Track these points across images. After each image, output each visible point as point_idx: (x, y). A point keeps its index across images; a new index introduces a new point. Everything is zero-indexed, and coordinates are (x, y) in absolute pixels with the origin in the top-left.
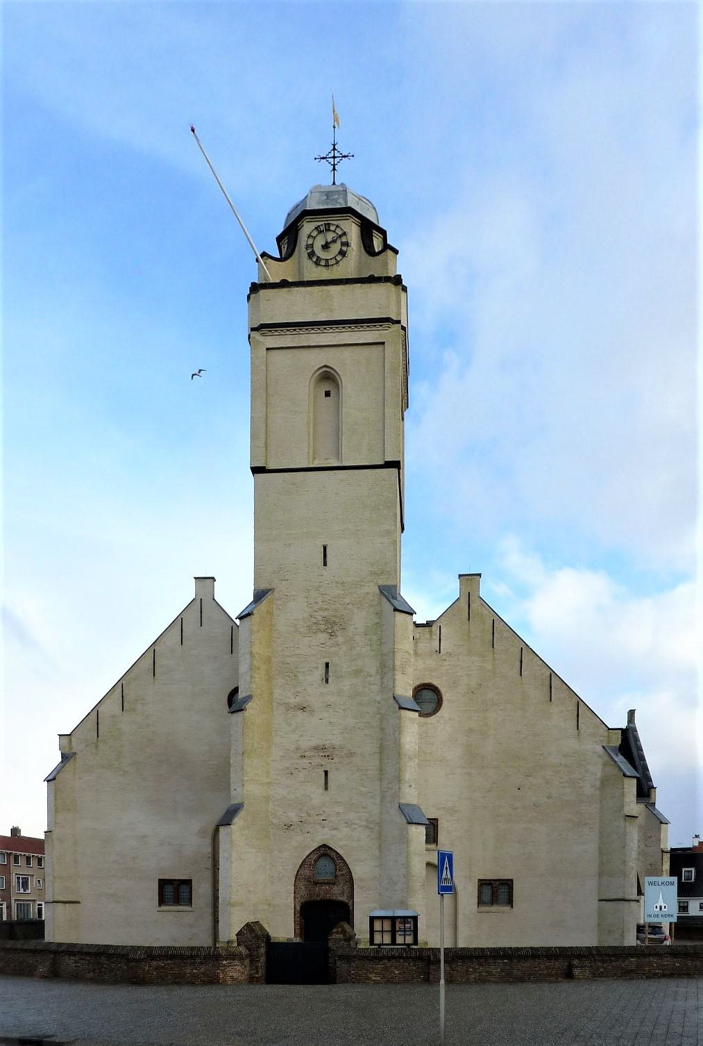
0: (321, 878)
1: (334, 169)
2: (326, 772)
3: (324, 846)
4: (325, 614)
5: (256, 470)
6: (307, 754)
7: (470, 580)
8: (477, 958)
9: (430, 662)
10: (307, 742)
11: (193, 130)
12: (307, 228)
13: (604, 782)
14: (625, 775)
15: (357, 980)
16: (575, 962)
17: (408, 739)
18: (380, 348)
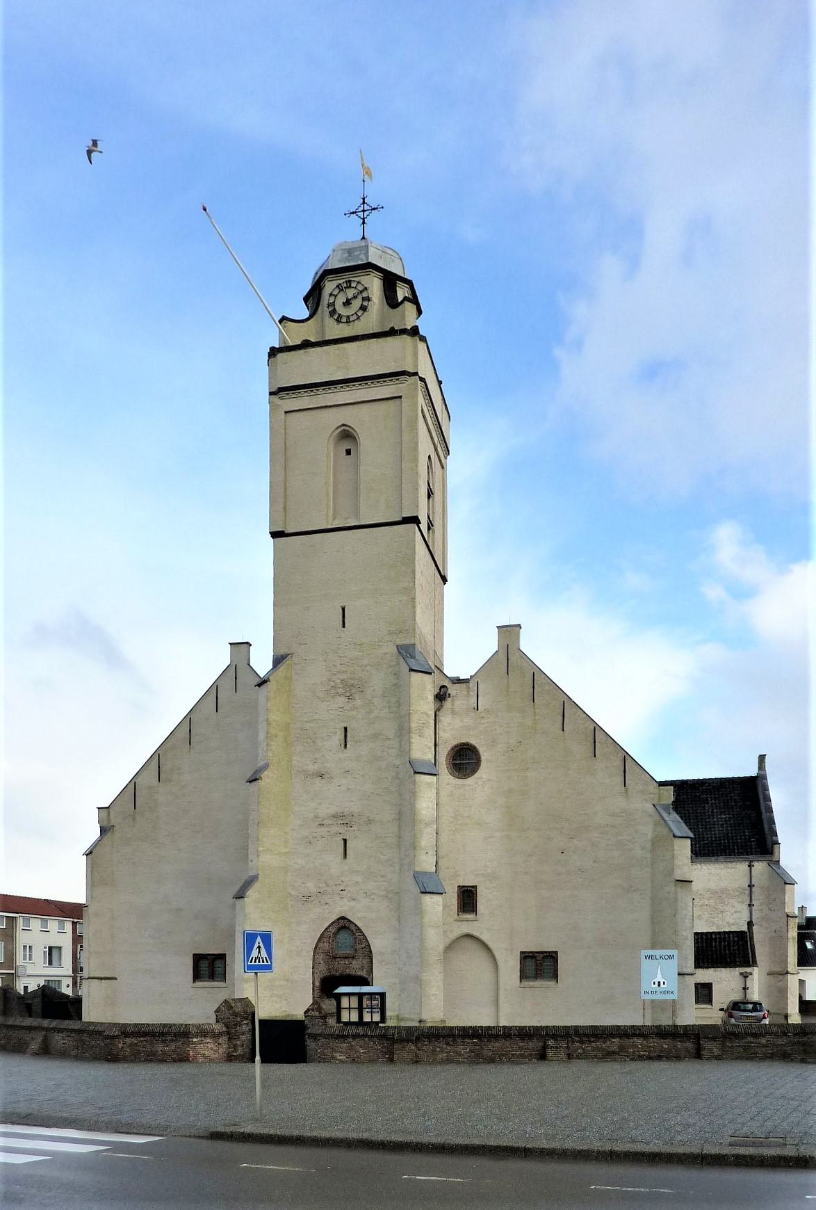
0: (340, 953)
2: (345, 840)
3: (343, 918)
4: (342, 677)
5: (275, 535)
6: (325, 822)
7: (509, 633)
8: (444, 1036)
10: (326, 810)
12: (330, 286)
13: (656, 843)
14: (674, 836)
15: (323, 1060)
16: (551, 1042)
17: (424, 805)
18: (398, 401)
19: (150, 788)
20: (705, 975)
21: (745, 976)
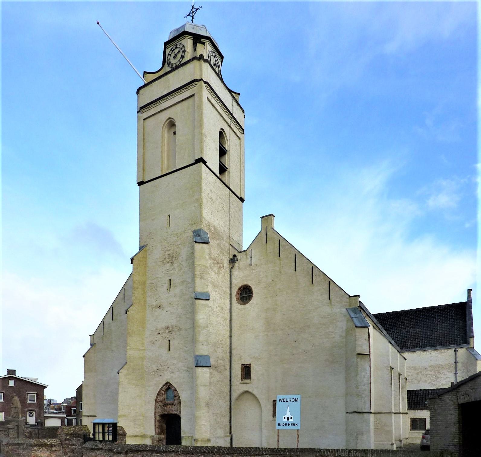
0: (168, 402)
2: (169, 341)
4: (168, 253)
5: (140, 184)
6: (161, 332)
7: (267, 219)
9: (246, 272)
10: (161, 326)
11: (98, 23)
13: (348, 332)
17: (201, 317)
19: (109, 324)
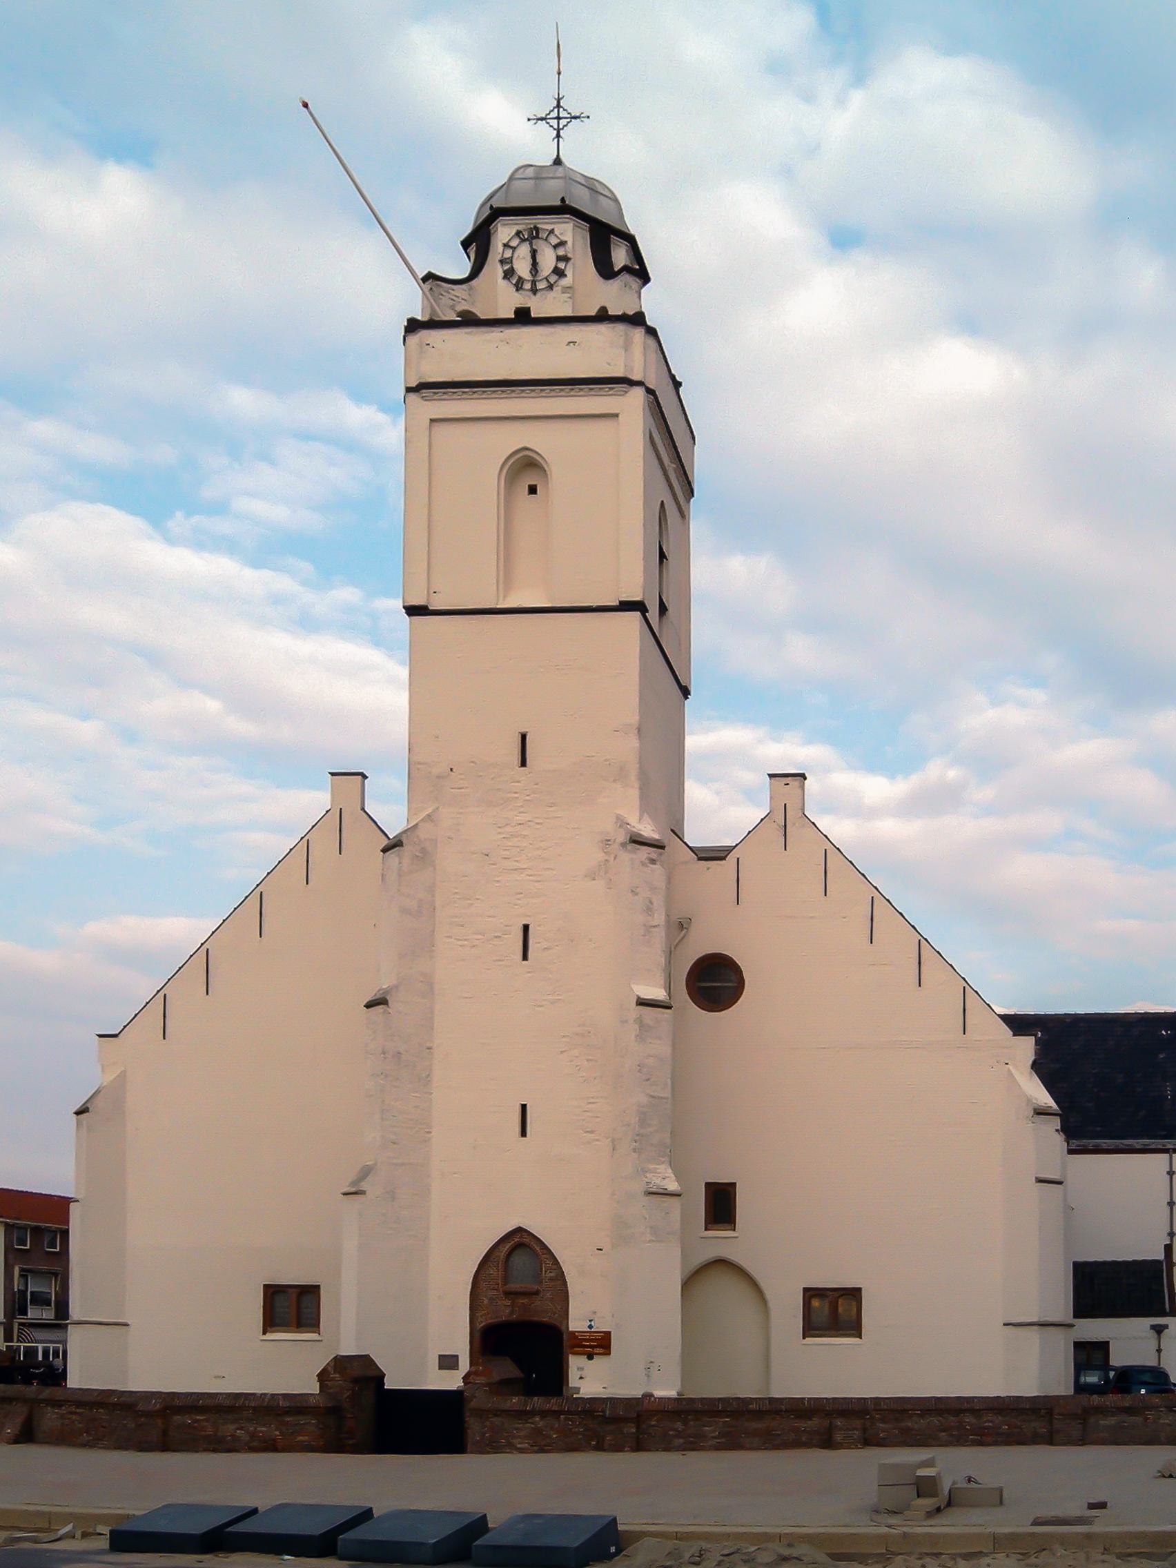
1: (558, 136)
12: (504, 232)
20: (1094, 1329)
21: (1159, 1330)
